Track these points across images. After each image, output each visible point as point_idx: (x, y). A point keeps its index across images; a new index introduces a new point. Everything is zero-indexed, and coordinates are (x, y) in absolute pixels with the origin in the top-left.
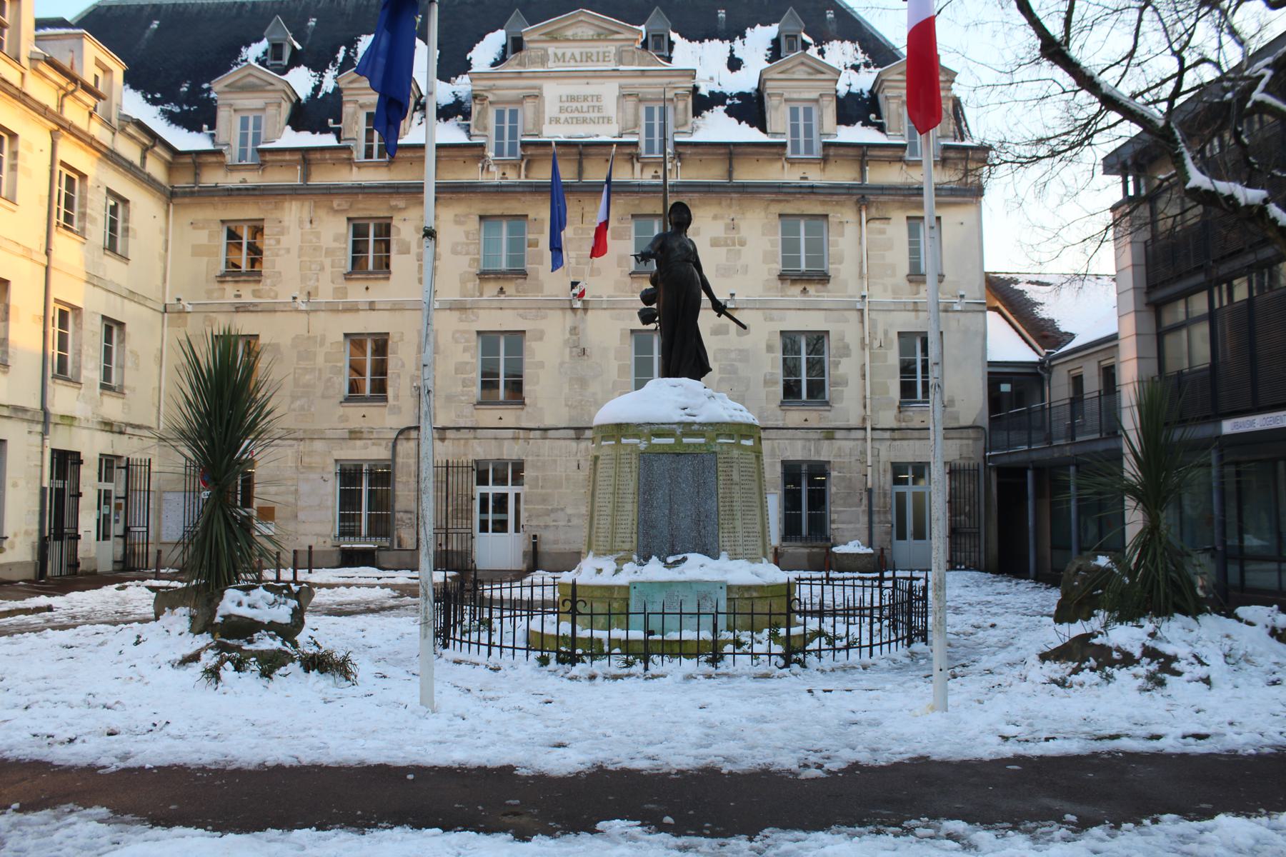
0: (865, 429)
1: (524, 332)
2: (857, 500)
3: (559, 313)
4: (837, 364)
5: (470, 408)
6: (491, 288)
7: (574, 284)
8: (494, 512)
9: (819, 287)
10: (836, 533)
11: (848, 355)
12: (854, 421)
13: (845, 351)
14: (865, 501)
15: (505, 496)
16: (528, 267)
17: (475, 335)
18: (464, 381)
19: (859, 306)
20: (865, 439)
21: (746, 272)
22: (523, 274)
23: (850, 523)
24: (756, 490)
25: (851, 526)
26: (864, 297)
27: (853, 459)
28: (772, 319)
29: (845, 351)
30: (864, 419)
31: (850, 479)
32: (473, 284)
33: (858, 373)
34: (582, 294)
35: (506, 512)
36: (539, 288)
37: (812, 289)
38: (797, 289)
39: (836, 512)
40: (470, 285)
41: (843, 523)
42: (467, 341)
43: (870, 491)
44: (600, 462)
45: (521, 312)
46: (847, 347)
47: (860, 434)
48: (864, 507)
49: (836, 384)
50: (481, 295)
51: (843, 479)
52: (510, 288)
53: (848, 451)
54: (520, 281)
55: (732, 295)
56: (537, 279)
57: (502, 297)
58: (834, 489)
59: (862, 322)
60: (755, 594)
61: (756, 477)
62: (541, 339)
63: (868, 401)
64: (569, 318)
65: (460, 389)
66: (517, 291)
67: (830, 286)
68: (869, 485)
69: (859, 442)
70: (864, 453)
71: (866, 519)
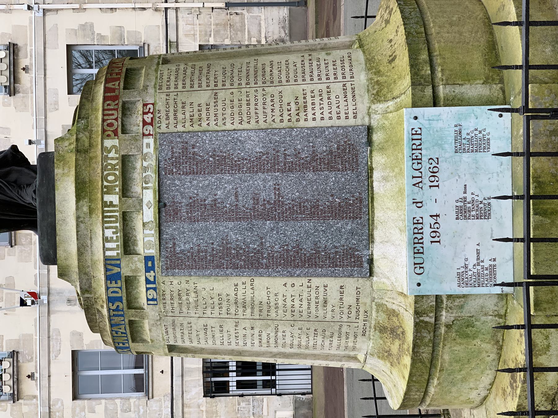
0: (166, 9)
1: (73, 352)
2: (237, 18)
3: (52, 317)
4: (102, 37)
5: (151, 402)
6: (28, 387)
7: (23, 303)
8: (254, 374)
9: (21, 54)
10: (270, 40)
11: (92, 26)
12: (159, 19)
13: (87, 28)
14: (239, 10)
15: (238, 382)
16: (6, 350)
17: (77, 402)
18: (125, 411)
19: (41, 14)
20: (177, 9)
21: (7, 128)
22: (14, 355)
23: (260, 24)
24: (226, 63)
25: (263, 23)
26: (29, 8)
27: (197, 22)
28: (56, 103)
29: (87, 28)
30: (156, 10)
31: (217, 25)
32: (24, 406)
33: (109, 14)
34: (33, 295)
35: (255, 363)
36: (27, 338)
37: (23, 62)
38: (24, 77)
39: (250, 39)
40: (25, 409)
41: (260, 31)
42: (83, 409)
43: (228, 5)
44: (179, 343)
45: (52, 355)
46: (83, 27)
47: (171, 14)
48: (244, 11)
49: (121, 37)
50: (35, 397)
51: (217, 32)
52: (27, 368)
53: (189, 27)
54: (20, 358)
55: (30, 142)
56: (18, 341)
57: (37, 375)
58: (227, 42)
59: (57, 10)
60: (424, 56)
61: (198, 64)
62: (80, 334)
63: (138, 6)
64: (59, 306)
65: (132, 414)
66: (30, 361)
67: (20, 43)
68: (223, 5)
69: (180, 15)
70: (190, 10)
71: (255, 8)
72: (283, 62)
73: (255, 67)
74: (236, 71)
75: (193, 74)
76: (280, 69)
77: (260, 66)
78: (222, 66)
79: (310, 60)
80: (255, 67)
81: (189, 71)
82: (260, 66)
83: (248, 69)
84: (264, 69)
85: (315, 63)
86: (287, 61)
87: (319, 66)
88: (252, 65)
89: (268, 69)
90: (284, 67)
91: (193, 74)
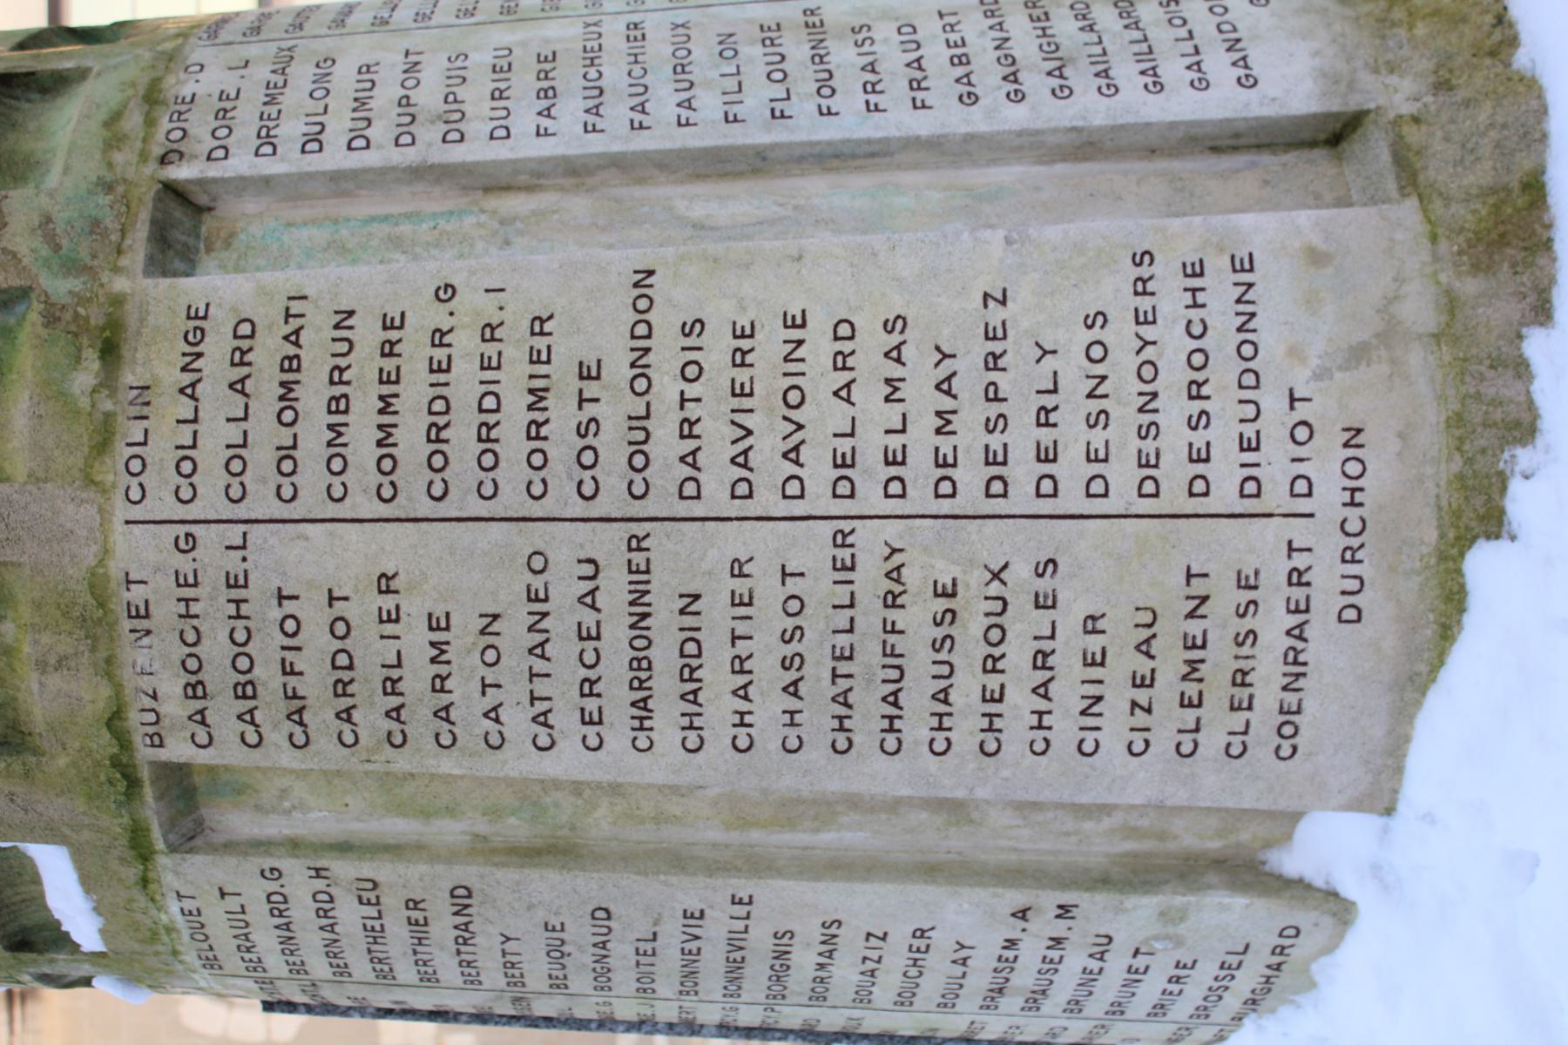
72: (900, 936)
73: (736, 943)
74: (621, 952)
75: (375, 935)
76: (870, 965)
77: (760, 939)
78: (541, 915)
79: (1057, 941)
80: (736, 943)
81: (349, 914)
82: (760, 939)
83: (693, 945)
84: (782, 955)
85: (1075, 961)
86: (920, 933)
87: (1089, 978)
88: (716, 930)
89: (804, 960)
90: (895, 960)
91: (375, 935)
